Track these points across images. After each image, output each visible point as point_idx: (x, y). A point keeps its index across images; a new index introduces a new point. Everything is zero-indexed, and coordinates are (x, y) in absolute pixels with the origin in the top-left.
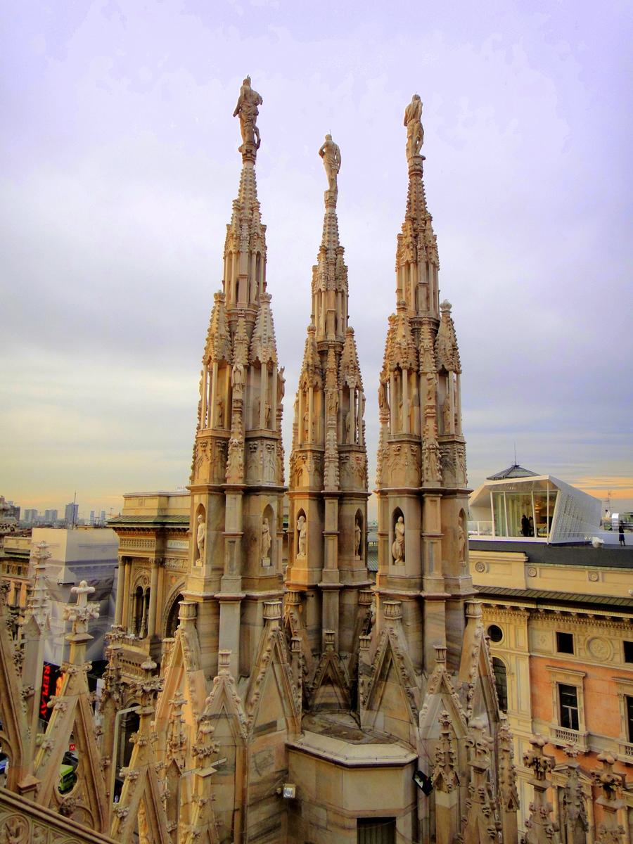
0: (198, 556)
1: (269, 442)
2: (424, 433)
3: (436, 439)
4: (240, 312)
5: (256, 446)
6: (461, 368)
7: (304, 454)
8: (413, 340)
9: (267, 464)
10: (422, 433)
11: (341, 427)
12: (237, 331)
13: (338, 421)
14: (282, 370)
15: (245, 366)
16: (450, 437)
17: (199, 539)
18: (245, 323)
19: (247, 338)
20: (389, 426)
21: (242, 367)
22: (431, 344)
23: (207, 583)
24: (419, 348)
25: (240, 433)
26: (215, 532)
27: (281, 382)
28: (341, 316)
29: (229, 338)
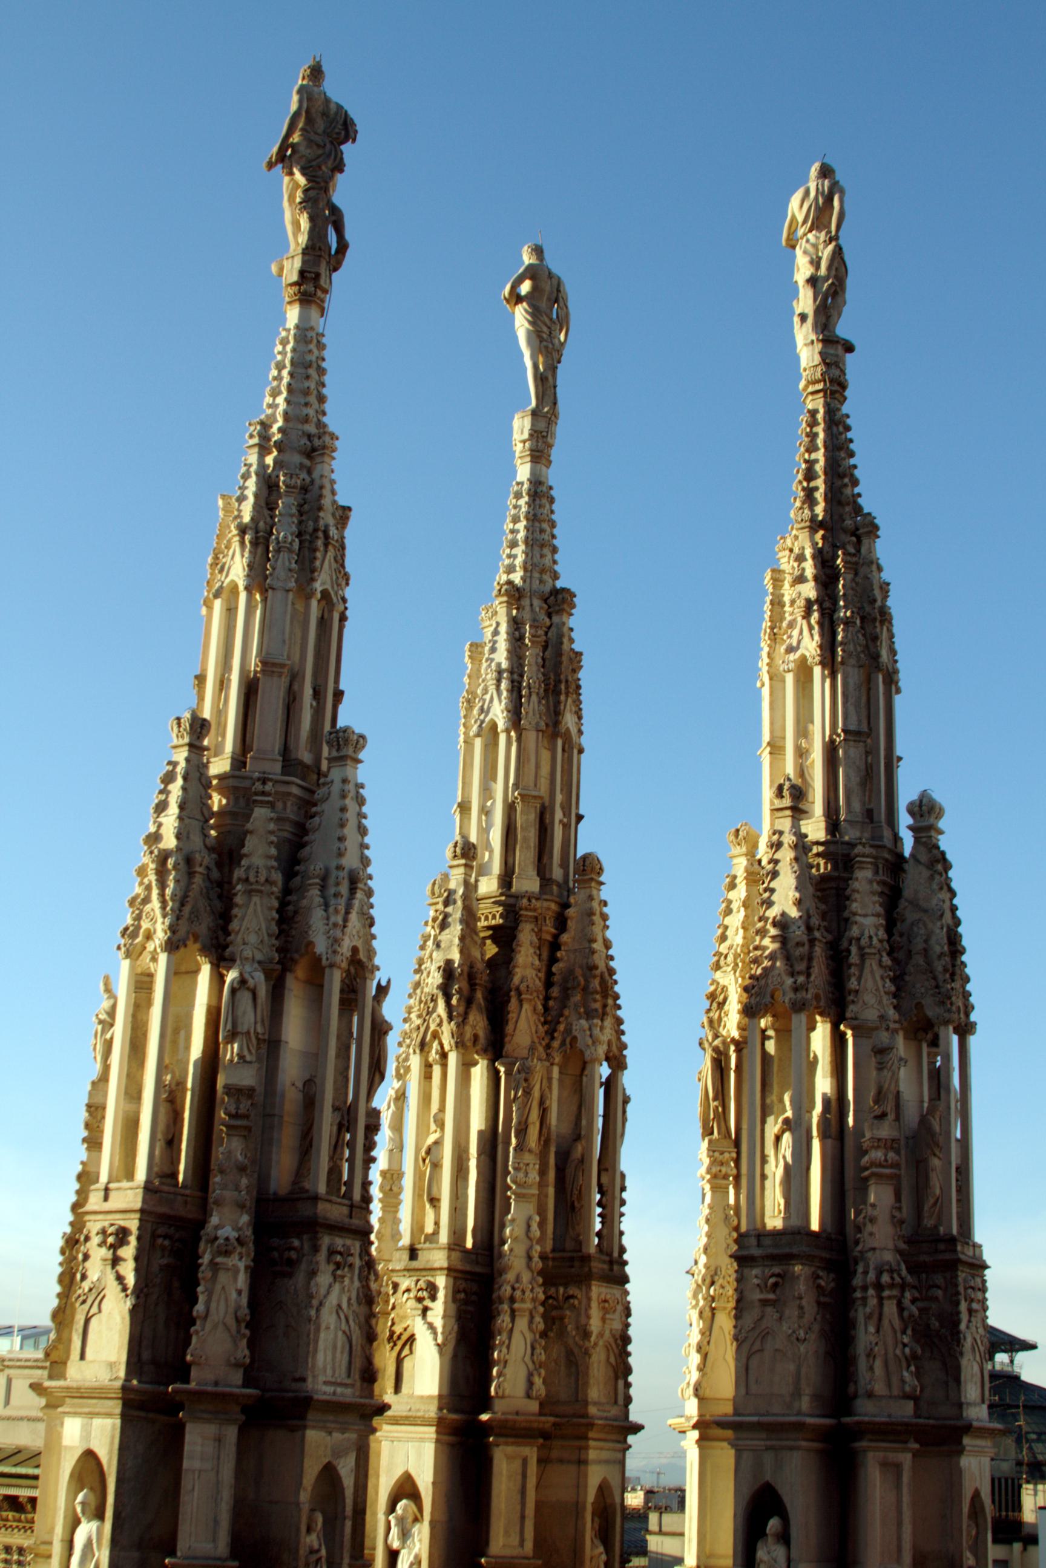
1: (339, 1242)
2: (859, 1229)
3: (900, 1252)
4: (258, 786)
5: (293, 1255)
6: (973, 1017)
8: (824, 916)
10: (850, 1230)
11: (551, 1191)
12: (245, 850)
13: (543, 1172)
14: (382, 991)
15: (268, 975)
16: (942, 1246)
18: (272, 826)
19: (278, 877)
20: (732, 1201)
21: (260, 976)
22: (882, 934)
24: (845, 944)
25: (241, 1206)
26: (136, 1555)
27: (380, 1029)
28: (559, 815)
29: (215, 874)
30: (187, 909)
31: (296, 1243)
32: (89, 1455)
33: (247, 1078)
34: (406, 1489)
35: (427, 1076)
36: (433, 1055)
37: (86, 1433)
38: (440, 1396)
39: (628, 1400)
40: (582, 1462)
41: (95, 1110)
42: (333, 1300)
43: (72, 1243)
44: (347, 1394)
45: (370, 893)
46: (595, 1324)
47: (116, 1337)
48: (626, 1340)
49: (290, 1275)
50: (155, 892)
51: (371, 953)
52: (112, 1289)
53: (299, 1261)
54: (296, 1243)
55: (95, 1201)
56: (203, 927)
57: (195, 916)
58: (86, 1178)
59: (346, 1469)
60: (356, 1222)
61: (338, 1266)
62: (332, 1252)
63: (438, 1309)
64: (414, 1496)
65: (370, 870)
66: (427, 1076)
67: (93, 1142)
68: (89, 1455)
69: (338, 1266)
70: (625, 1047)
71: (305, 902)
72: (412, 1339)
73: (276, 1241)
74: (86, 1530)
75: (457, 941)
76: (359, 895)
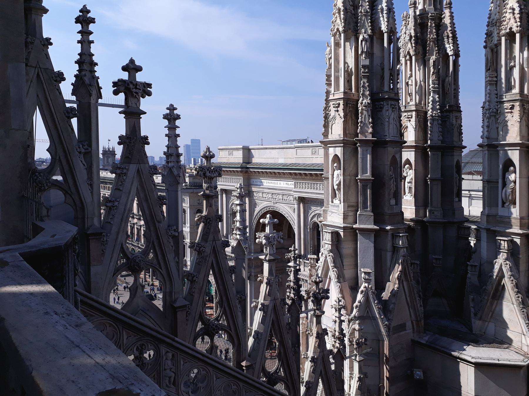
0: (334, 196)
5: (382, 106)
7: (409, 114)
9: (391, 121)
17: (336, 183)
23: (345, 217)
30: (347, 22)
31: (382, 103)
32: (336, 156)
33: (367, 62)
34: (408, 162)
35: (406, 64)
36: (408, 57)
37: (335, 151)
38: (415, 141)
39: (462, 141)
40: (453, 155)
41: (329, 76)
42: (392, 116)
43: (326, 109)
44: (397, 139)
45: (394, 13)
46: (454, 121)
47: (340, 128)
48: (462, 126)
49: (381, 111)
50: (338, 18)
51: (396, 29)
52: (338, 117)
53: (383, 108)
54: (382, 103)
55: (331, 97)
56: (351, 27)
57: (349, 23)
58: (328, 93)
59: (397, 156)
60: (396, 97)
61: (393, 108)
62: (391, 105)
63: (413, 119)
64: (410, 164)
65: (393, 6)
66: (406, 64)
67: (329, 85)
68: (336, 156)
69: (393, 108)
70: (460, 51)
71: (377, 17)
72: (407, 127)
73: (377, 103)
74: (337, 172)
75: (413, 27)
76: (392, 13)
